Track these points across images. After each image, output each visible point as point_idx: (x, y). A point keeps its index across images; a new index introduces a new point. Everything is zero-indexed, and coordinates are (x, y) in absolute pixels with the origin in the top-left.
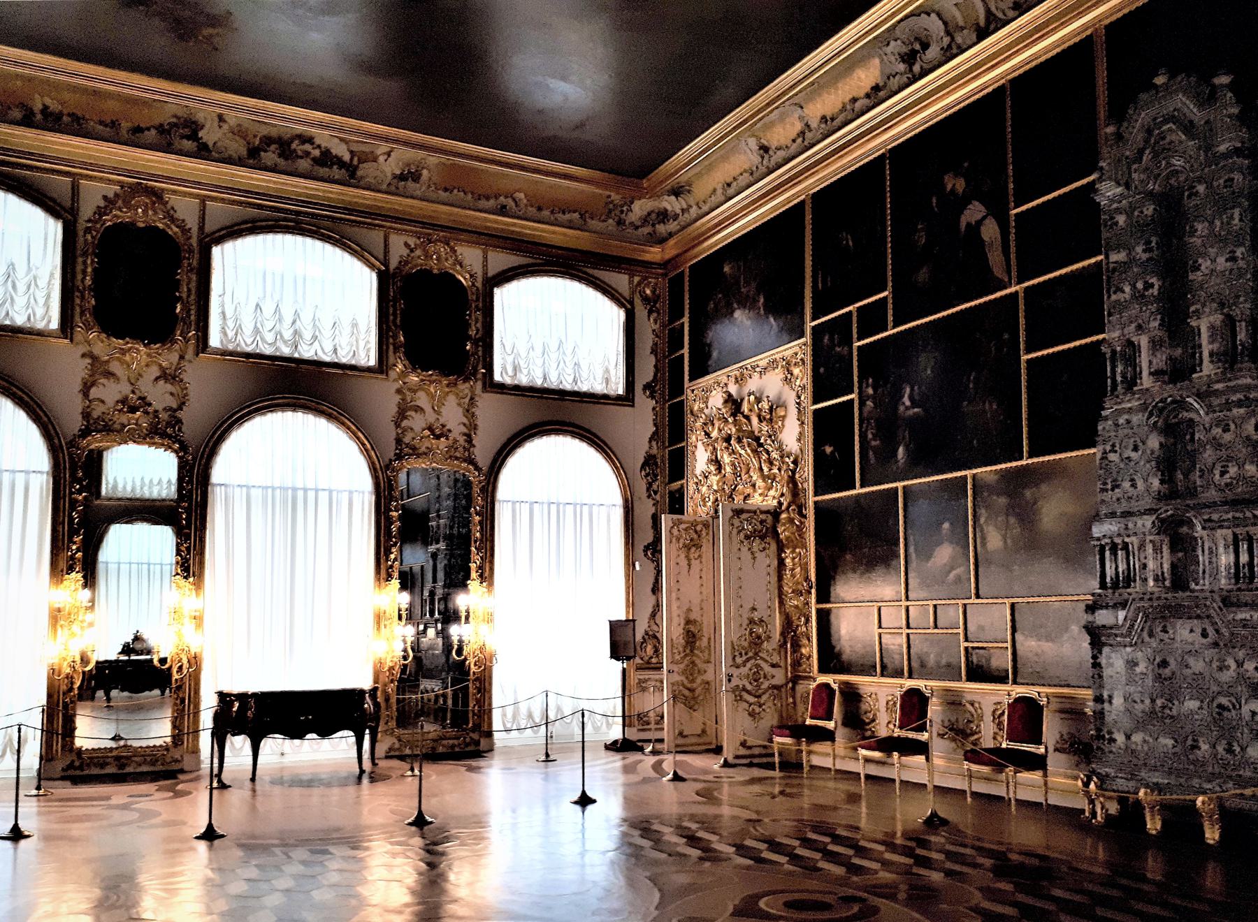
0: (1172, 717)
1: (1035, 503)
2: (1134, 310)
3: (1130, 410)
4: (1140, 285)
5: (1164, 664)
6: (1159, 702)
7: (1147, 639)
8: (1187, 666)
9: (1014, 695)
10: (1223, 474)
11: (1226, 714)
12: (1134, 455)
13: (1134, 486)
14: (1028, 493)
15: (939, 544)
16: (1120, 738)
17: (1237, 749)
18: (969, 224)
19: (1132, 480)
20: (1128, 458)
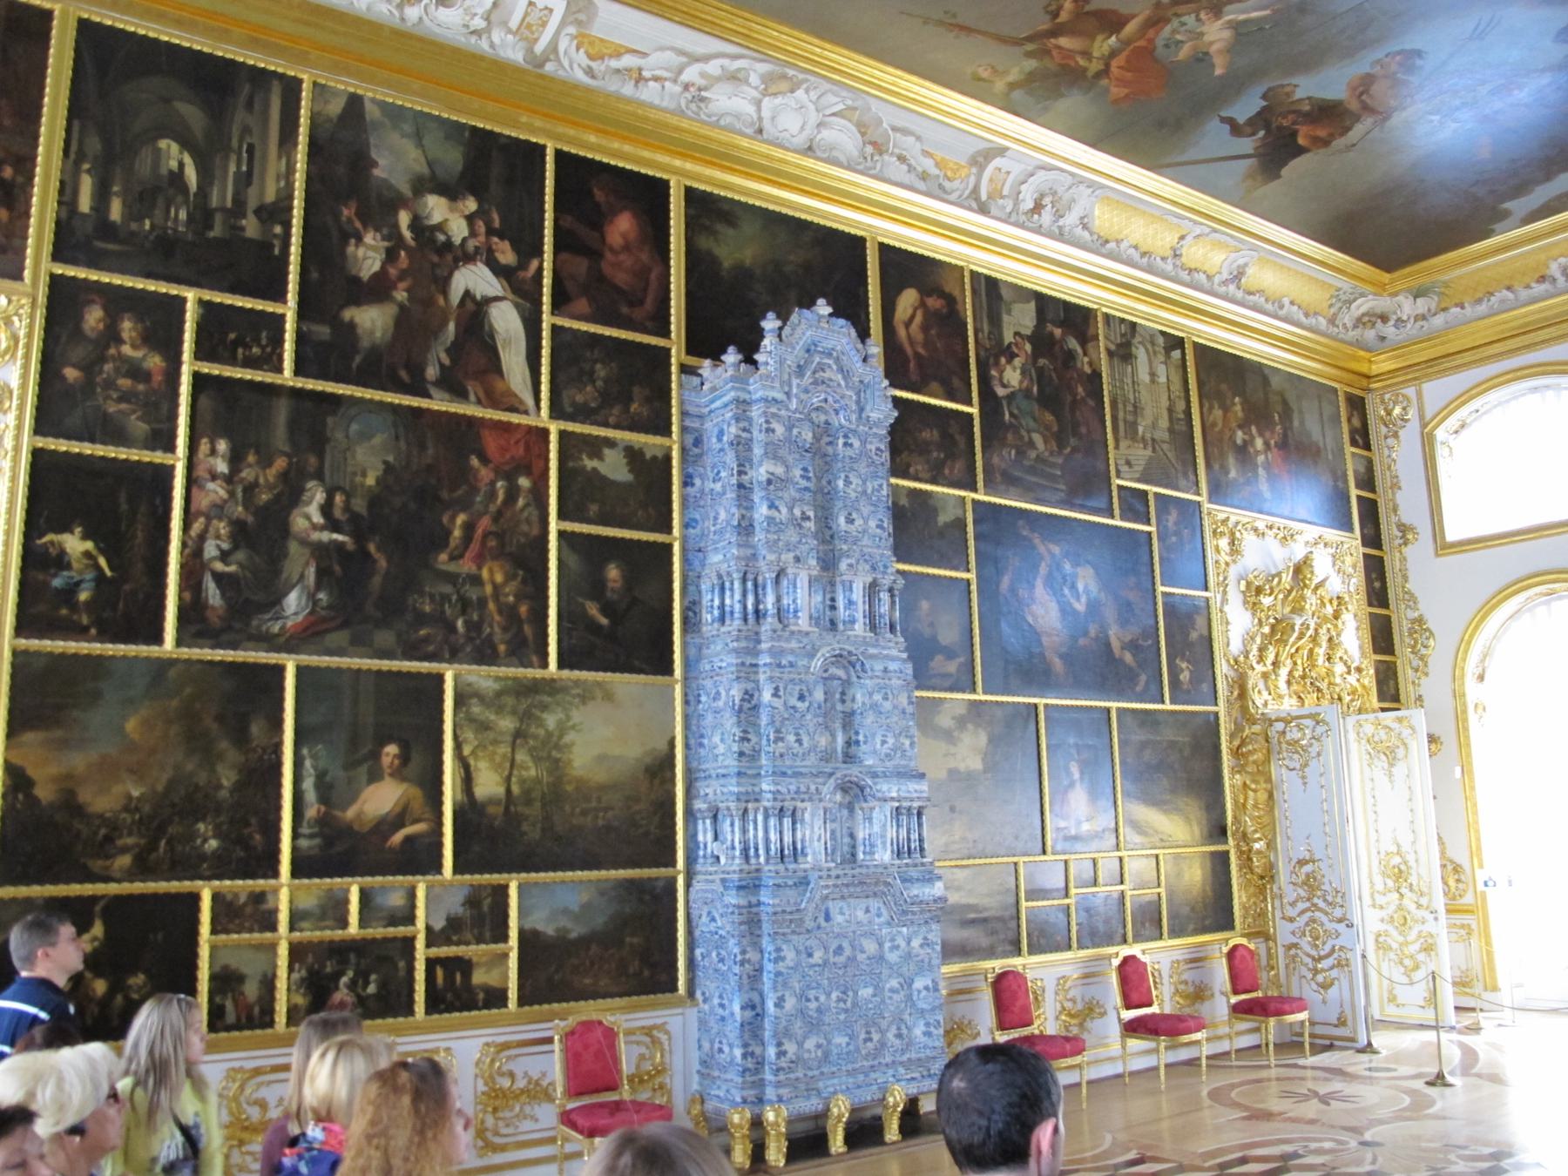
0: (846, 1011)
1: (561, 737)
2: (791, 535)
3: (792, 651)
4: (797, 512)
5: (840, 948)
6: (834, 996)
7: (823, 924)
8: (863, 952)
9: (571, 1021)
10: (884, 742)
11: (895, 996)
12: (799, 704)
13: (799, 741)
14: (551, 720)
15: (375, 776)
16: (791, 1048)
17: (905, 1031)
18: (467, 294)
19: (797, 734)
20: (793, 707)
